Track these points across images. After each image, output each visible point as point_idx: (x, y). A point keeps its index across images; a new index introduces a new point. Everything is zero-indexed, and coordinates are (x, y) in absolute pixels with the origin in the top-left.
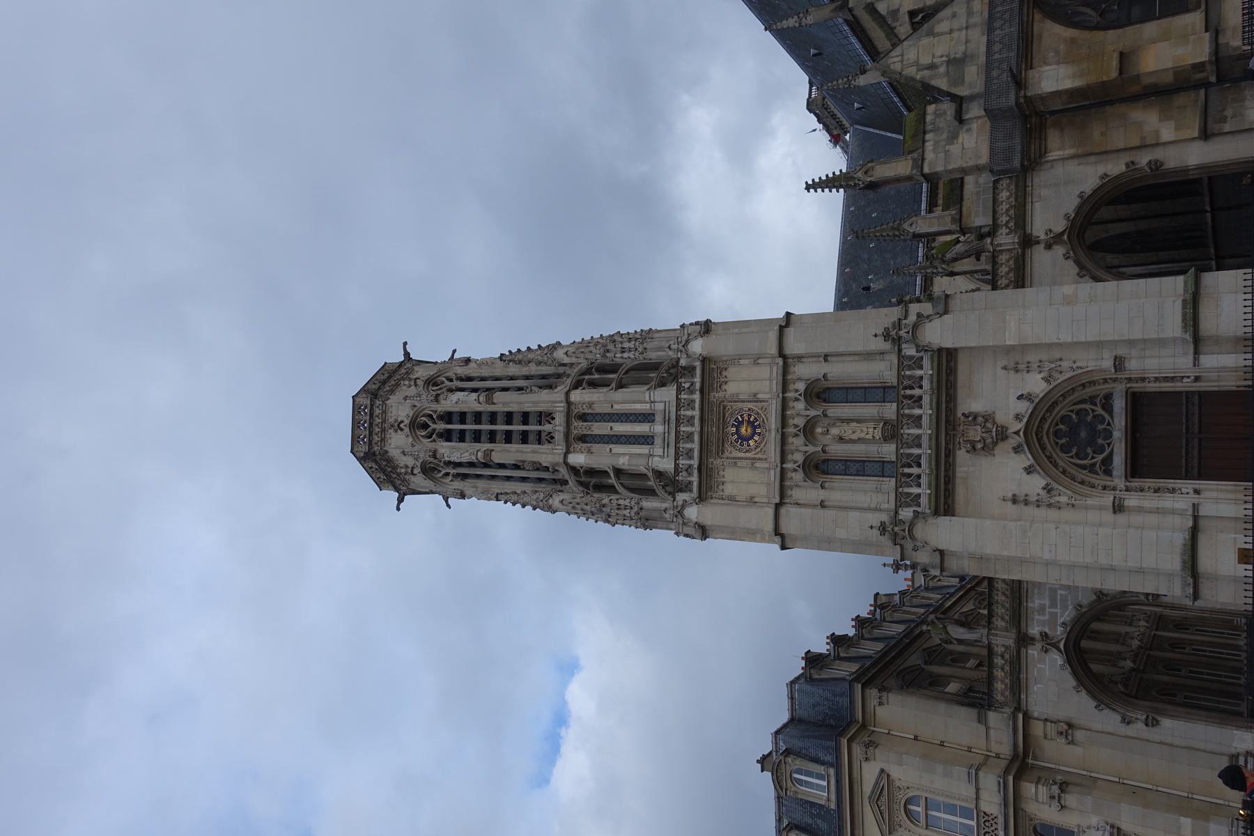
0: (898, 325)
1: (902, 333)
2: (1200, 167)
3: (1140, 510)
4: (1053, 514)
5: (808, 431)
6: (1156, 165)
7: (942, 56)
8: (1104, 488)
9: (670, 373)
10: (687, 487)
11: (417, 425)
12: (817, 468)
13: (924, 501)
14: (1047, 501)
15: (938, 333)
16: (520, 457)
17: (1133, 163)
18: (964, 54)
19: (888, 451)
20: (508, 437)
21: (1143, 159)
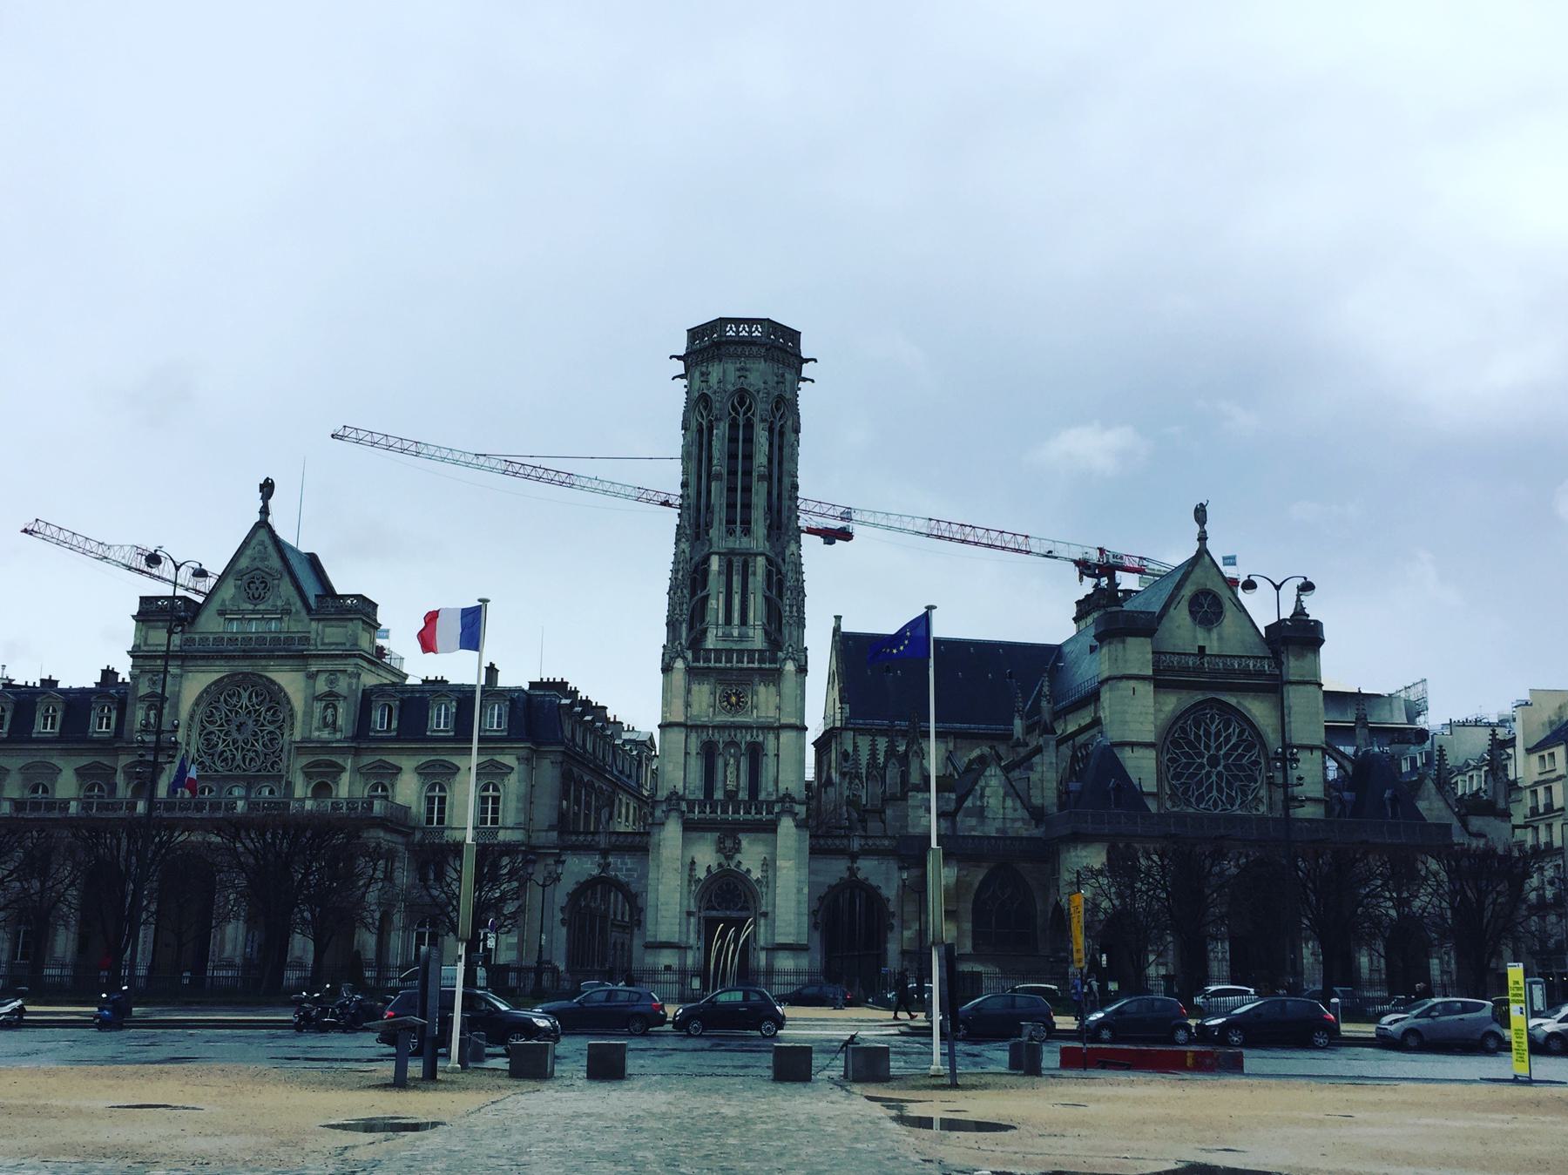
0: (793, 800)
1: (787, 805)
2: (886, 950)
3: (688, 924)
4: (686, 883)
5: (732, 743)
6: (891, 927)
7: (988, 803)
8: (700, 907)
9: (775, 641)
10: (696, 659)
11: (742, 396)
12: (709, 753)
13: (691, 816)
14: (692, 879)
15: (787, 824)
16: (717, 509)
17: (894, 915)
18: (986, 817)
19: (719, 795)
20: (732, 490)
21: (895, 922)
